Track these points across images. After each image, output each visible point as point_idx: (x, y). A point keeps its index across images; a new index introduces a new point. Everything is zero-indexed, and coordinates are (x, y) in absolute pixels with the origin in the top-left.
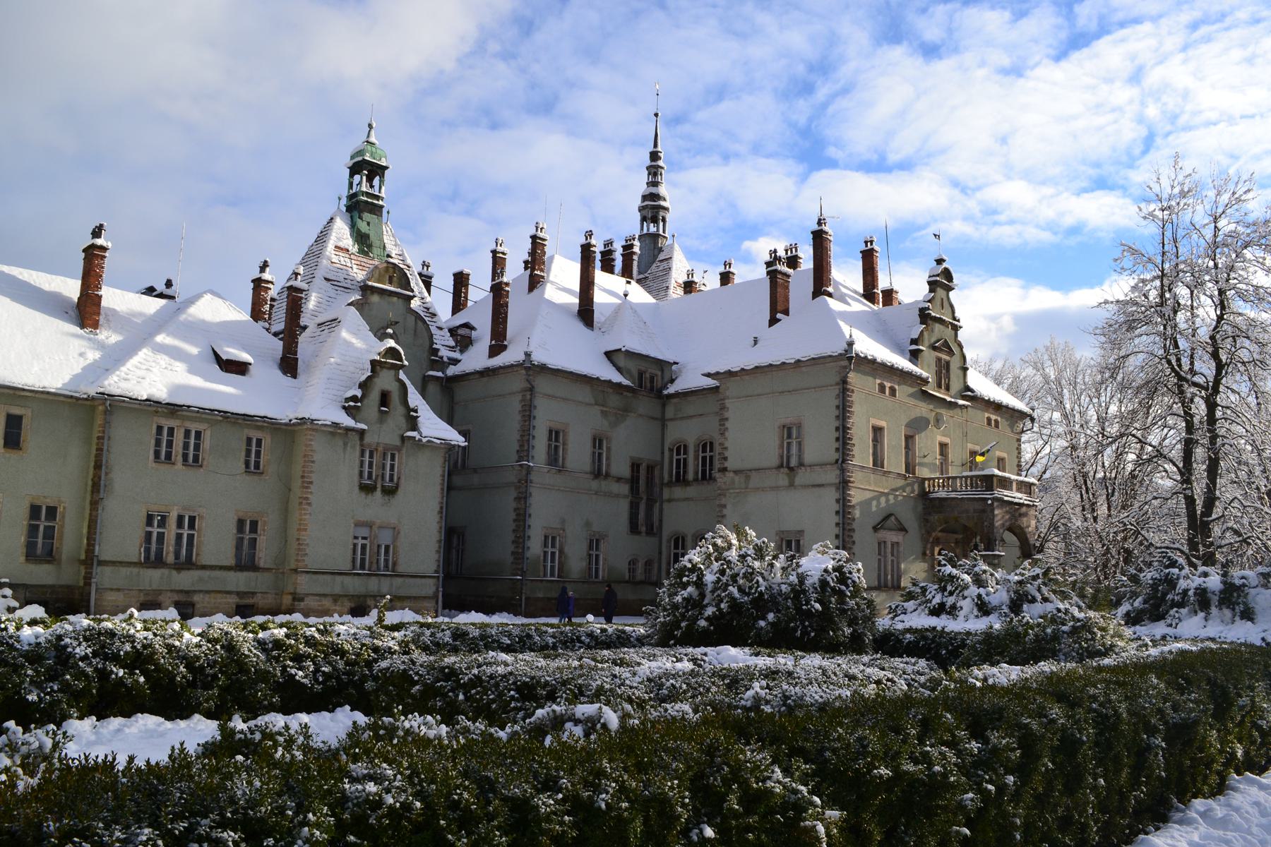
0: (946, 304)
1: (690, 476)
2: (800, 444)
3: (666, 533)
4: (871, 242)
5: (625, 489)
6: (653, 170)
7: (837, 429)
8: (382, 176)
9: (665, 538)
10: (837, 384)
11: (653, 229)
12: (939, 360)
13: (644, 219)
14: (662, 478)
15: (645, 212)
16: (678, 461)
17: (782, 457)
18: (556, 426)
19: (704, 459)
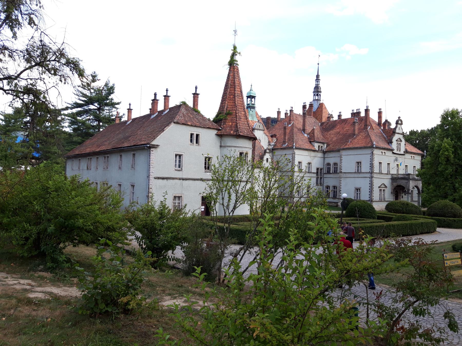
0: (400, 128)
1: (331, 172)
2: (361, 166)
3: (325, 185)
4: (381, 109)
5: (315, 175)
6: (317, 81)
7: (370, 164)
8: (255, 99)
9: (324, 187)
10: (371, 153)
11: (317, 98)
12: (397, 143)
13: (314, 95)
14: (324, 172)
15: (315, 93)
16: (328, 168)
17: (356, 170)
18: (300, 161)
19: (335, 167)
